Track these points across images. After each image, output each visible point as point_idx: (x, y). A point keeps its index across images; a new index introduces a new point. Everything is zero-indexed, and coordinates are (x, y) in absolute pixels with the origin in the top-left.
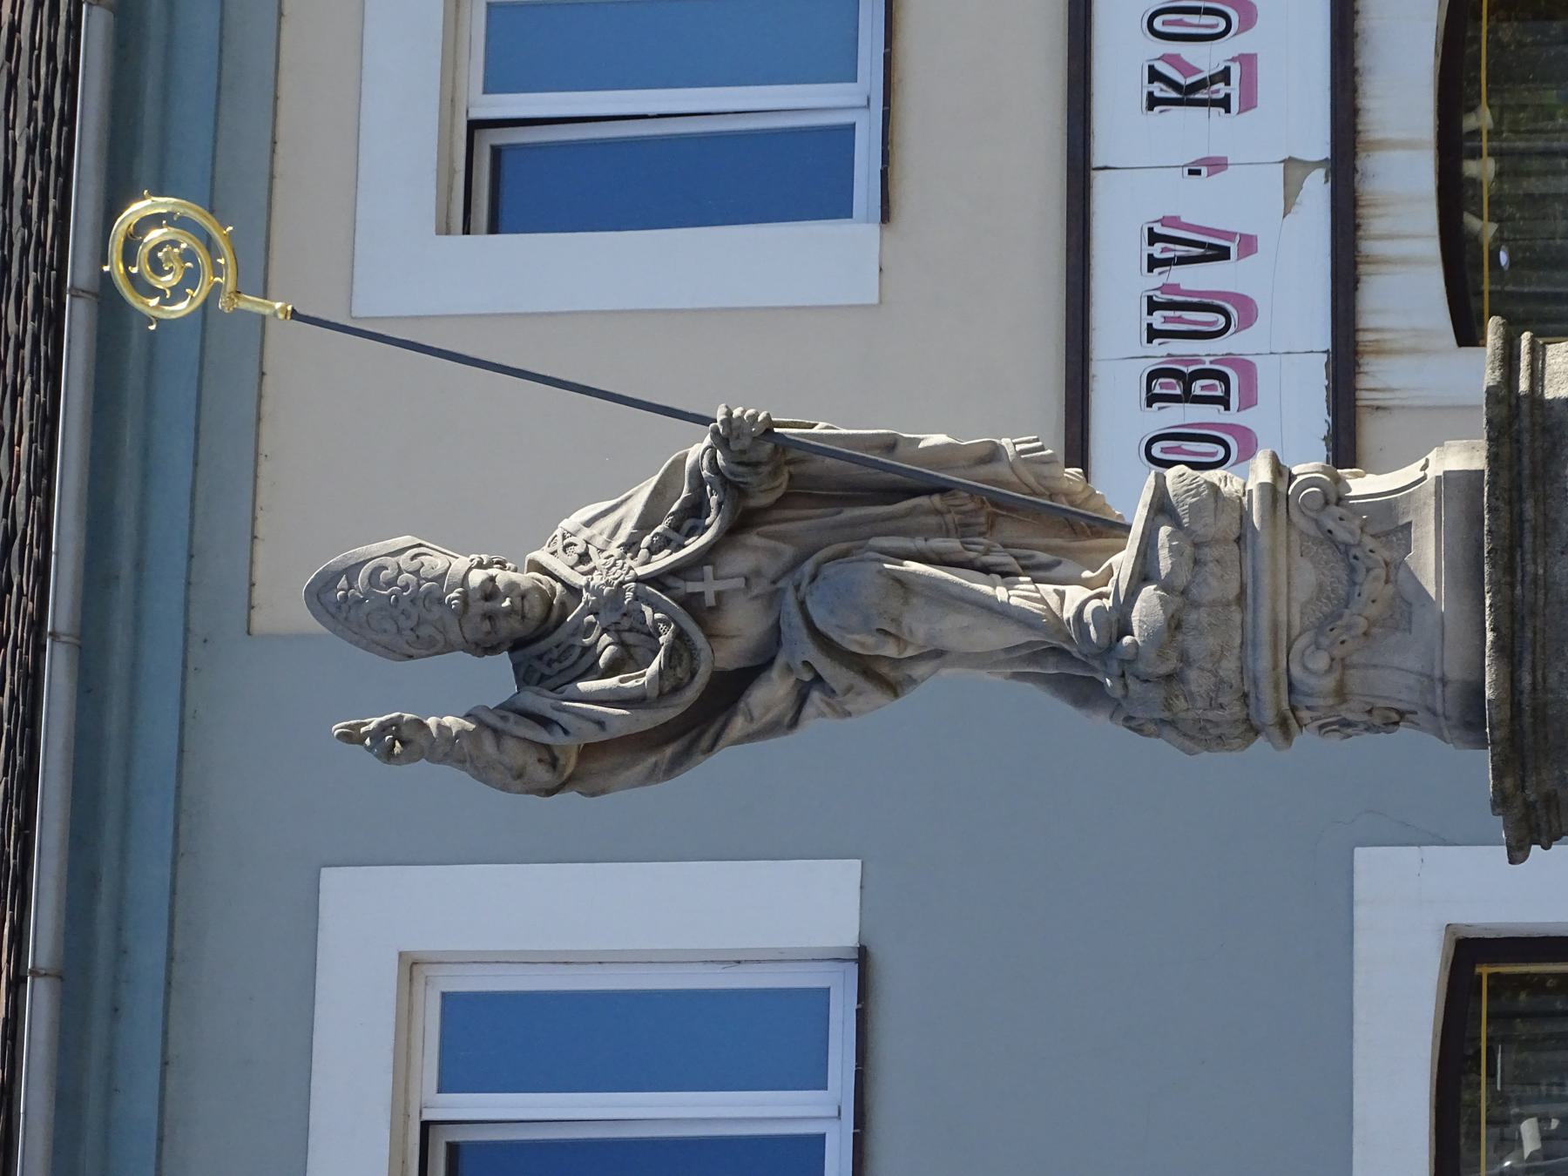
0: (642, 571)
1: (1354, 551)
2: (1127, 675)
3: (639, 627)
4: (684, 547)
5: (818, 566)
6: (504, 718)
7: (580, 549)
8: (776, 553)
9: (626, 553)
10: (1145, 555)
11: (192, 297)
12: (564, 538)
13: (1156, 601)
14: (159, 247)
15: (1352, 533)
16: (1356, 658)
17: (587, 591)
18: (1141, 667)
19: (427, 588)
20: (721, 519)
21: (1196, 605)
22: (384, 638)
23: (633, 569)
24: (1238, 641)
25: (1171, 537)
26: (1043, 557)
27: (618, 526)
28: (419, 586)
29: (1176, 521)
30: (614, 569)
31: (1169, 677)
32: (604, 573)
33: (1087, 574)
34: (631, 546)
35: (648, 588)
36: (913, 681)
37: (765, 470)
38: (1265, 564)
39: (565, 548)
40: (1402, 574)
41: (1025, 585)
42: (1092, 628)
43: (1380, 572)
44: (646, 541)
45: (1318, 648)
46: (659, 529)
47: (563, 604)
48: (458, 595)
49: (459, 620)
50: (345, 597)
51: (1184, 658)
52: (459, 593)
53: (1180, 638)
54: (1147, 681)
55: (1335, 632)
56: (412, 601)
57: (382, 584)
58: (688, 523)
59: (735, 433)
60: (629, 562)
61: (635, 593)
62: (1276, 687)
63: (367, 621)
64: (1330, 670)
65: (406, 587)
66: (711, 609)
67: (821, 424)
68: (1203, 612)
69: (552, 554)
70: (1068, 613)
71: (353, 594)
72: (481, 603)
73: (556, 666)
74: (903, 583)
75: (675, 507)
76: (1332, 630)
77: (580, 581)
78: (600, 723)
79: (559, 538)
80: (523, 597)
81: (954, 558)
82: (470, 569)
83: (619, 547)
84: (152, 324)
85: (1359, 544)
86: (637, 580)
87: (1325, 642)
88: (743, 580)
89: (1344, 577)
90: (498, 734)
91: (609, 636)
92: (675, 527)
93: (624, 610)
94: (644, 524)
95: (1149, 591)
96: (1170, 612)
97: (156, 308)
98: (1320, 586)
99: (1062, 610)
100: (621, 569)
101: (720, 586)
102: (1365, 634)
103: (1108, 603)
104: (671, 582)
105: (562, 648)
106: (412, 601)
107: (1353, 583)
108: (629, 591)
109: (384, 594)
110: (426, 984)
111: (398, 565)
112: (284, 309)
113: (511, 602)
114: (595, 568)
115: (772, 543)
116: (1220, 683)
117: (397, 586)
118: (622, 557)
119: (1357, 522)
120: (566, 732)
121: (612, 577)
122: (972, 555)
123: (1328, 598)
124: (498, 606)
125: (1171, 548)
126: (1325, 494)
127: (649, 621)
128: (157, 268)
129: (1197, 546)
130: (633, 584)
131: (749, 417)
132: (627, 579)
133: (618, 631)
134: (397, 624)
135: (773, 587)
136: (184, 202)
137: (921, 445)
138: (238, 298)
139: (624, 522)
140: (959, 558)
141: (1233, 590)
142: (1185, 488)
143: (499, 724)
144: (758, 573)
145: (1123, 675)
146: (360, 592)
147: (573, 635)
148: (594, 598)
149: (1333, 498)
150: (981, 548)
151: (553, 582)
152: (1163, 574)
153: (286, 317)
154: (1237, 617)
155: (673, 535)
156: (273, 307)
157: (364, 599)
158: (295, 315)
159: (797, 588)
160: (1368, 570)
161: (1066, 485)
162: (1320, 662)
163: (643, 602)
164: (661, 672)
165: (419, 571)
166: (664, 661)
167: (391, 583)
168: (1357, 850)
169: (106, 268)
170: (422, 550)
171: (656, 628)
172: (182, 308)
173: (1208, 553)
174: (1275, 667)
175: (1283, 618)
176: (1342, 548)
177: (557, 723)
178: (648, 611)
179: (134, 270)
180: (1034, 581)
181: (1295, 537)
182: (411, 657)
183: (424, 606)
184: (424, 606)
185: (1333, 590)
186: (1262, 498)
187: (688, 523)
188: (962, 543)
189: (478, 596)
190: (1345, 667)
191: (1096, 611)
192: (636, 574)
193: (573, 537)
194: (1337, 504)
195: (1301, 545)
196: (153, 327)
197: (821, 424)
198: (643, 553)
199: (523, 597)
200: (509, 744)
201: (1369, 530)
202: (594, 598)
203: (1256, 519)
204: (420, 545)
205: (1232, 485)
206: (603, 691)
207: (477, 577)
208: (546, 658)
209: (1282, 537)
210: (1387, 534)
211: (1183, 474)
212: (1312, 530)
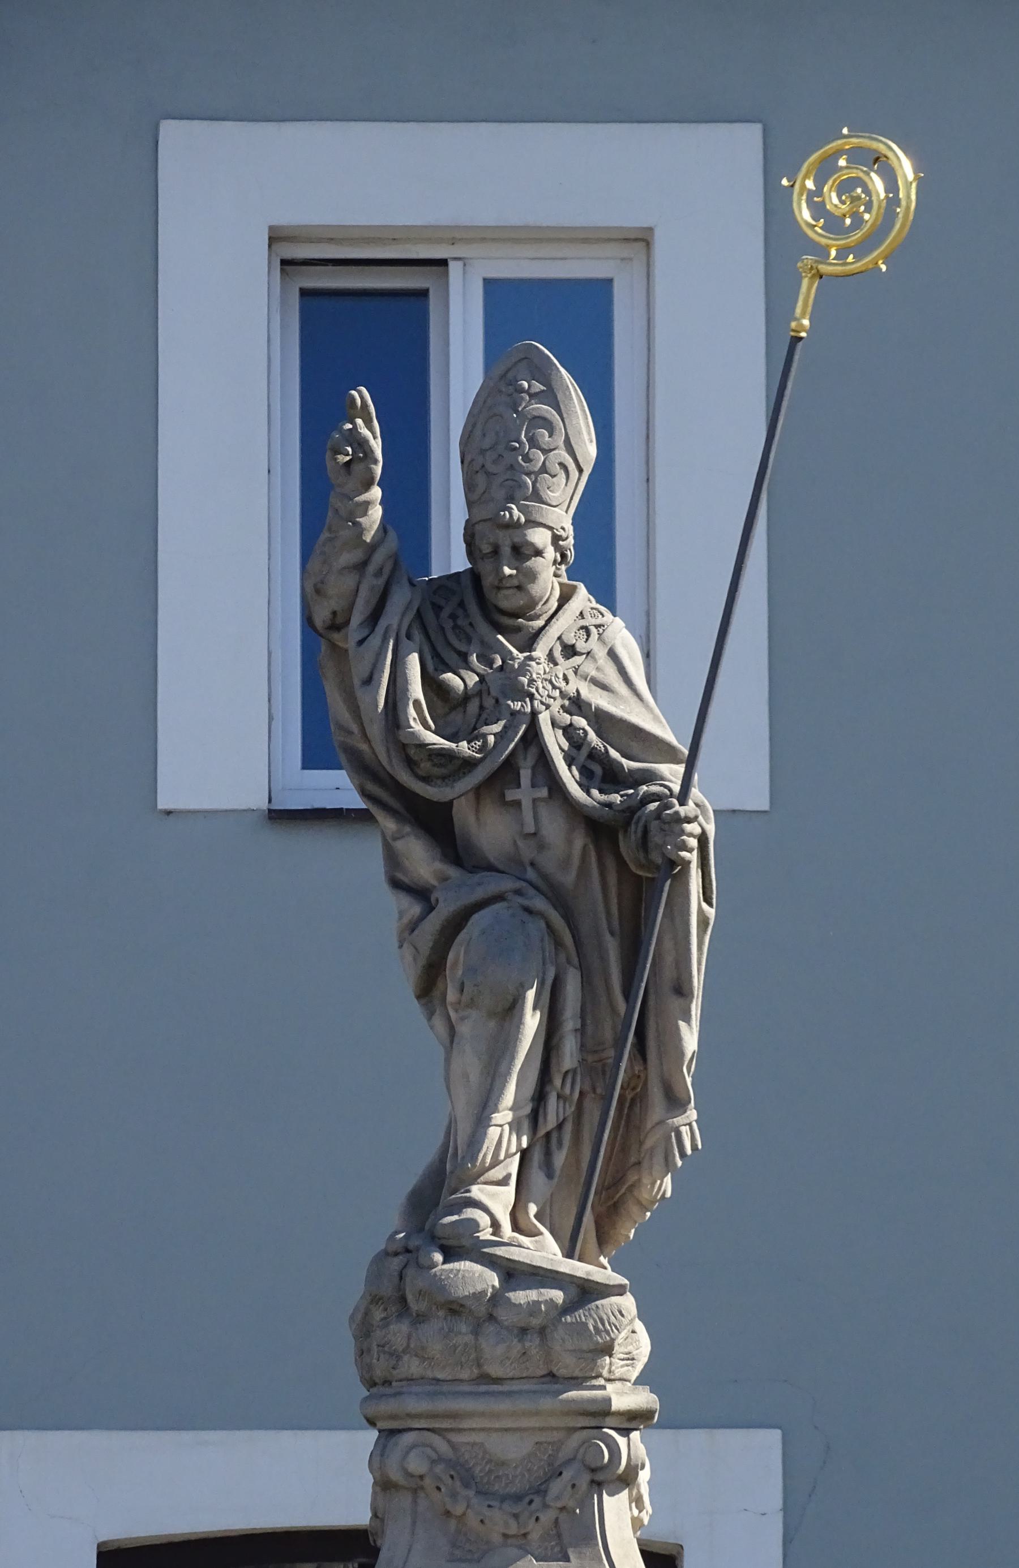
1: (537, 1500)
2: (408, 1255)
3: (484, 716)
4: (569, 766)
5: (541, 915)
6: (379, 573)
7: (581, 646)
9: (570, 699)
10: (534, 1274)
11: (815, 226)
12: (597, 626)
13: (479, 1288)
14: (867, 191)
15: (558, 1498)
16: (423, 1503)
17: (526, 658)
18: (410, 1272)
19: (525, 483)
20: (594, 807)
21: (476, 1332)
22: (478, 432)
23: (546, 709)
24: (440, 1376)
25: (551, 1302)
26: (560, 1158)
27: (604, 687)
28: (528, 474)
29: (569, 1308)
30: (550, 687)
31: (403, 1300)
32: (545, 676)
33: (533, 1209)
34: (577, 705)
35: (524, 727)
36: (430, 1015)
37: (641, 856)
38: (523, 1404)
39: (586, 629)
40: (513, 1552)
41: (515, 1143)
42: (455, 1218)
43: (513, 1529)
44: (581, 722)
45: (433, 1462)
46: (592, 736)
47: (519, 629)
48: (515, 518)
49: (490, 519)
50: (522, 390)
51: (420, 1319)
52: (519, 519)
53: (441, 1313)
54: (401, 1277)
55: (450, 1481)
56: (512, 466)
57: (533, 431)
58: (598, 770)
59: (666, 827)
60: (556, 706)
62: (393, 1417)
63: (495, 415)
64: (409, 1475)
65: (527, 459)
66: (503, 795)
67: (711, 912)
68: (469, 1338)
69: (581, 613)
70: (476, 1191)
71: (522, 398)
72: (508, 542)
73: (448, 625)
74: (512, 1010)
75: (614, 754)
76: (452, 1477)
77: (540, 652)
78: (370, 680)
79: (599, 620)
80: (519, 588)
81: (554, 1061)
82: (550, 528)
83: (578, 691)
84: (789, 181)
85: (546, 1506)
86: (534, 714)
87: (439, 1469)
88: (532, 831)
89: (512, 1489)
90: (361, 566)
91: (476, 683)
92: (593, 755)
93: (501, 700)
94: (601, 720)
95: (493, 1279)
96: (468, 1303)
97: (803, 186)
98: (503, 1464)
99: (486, 1183)
100: (549, 696)
102: (448, 1513)
103: (486, 1235)
104: (533, 751)
105: (469, 629)
106: (512, 466)
107: (503, 1499)
108: (522, 706)
109: (520, 434)
110: (623, 259)
113: (510, 576)
114: (556, 664)
115: (576, 861)
116: (396, 1356)
117: (529, 449)
118: (563, 695)
119: (571, 1504)
120: (361, 642)
121: (540, 686)
122: (558, 1082)
123: (490, 1471)
124: (505, 562)
125: (537, 1303)
126: (603, 1468)
127: (485, 729)
128: (845, 188)
129: (542, 1331)
130: (528, 709)
131: (683, 841)
132: (536, 703)
133: (479, 694)
134: (490, 448)
135: (527, 861)
136: (911, 217)
137: (682, 1024)
138: (813, 276)
139: (610, 694)
140: (554, 1069)
141: (494, 1370)
142: (605, 1317)
143: (371, 568)
144: (542, 847)
145: (408, 1251)
146: (525, 407)
147: (483, 643)
148: (516, 666)
149: (600, 1477)
150: (567, 1090)
151: (546, 617)
152: (511, 1295)
153: (793, 331)
154: (465, 1375)
155: (584, 752)
156: (803, 316)
157: (516, 412)
159: (518, 892)
160: (516, 1516)
161: (646, 1180)
162: (416, 1464)
163: (508, 721)
164: (423, 746)
165: (547, 473)
166: (436, 749)
167: (533, 442)
168: (776, 1435)
169: (845, 131)
170: (574, 473)
171: (477, 738)
172: (906, 168)
173: (532, 1344)
174: (410, 1416)
175: (466, 1424)
176: (543, 1487)
177: (372, 631)
178: (497, 728)
179: (842, 162)
180: (525, 1154)
181: (556, 1436)
182: (462, 462)
183: (507, 480)
185: (497, 1477)
186: (593, 1401)
187: (598, 770)
188: (574, 1071)
189: (516, 540)
190: (415, 1491)
191: (474, 1225)
192: (540, 713)
193: (597, 636)
194: (593, 1482)
195: (549, 1443)
196: (785, 182)
197: (711, 912)
198: (566, 718)
200: (349, 581)
201: (563, 1517)
202: (516, 666)
203: (573, 1394)
204: (581, 471)
205: (622, 1366)
206: (406, 682)
207: (540, 537)
208: (460, 612)
209: (554, 1422)
210: (559, 1536)
211: (623, 1315)
212: (563, 1455)
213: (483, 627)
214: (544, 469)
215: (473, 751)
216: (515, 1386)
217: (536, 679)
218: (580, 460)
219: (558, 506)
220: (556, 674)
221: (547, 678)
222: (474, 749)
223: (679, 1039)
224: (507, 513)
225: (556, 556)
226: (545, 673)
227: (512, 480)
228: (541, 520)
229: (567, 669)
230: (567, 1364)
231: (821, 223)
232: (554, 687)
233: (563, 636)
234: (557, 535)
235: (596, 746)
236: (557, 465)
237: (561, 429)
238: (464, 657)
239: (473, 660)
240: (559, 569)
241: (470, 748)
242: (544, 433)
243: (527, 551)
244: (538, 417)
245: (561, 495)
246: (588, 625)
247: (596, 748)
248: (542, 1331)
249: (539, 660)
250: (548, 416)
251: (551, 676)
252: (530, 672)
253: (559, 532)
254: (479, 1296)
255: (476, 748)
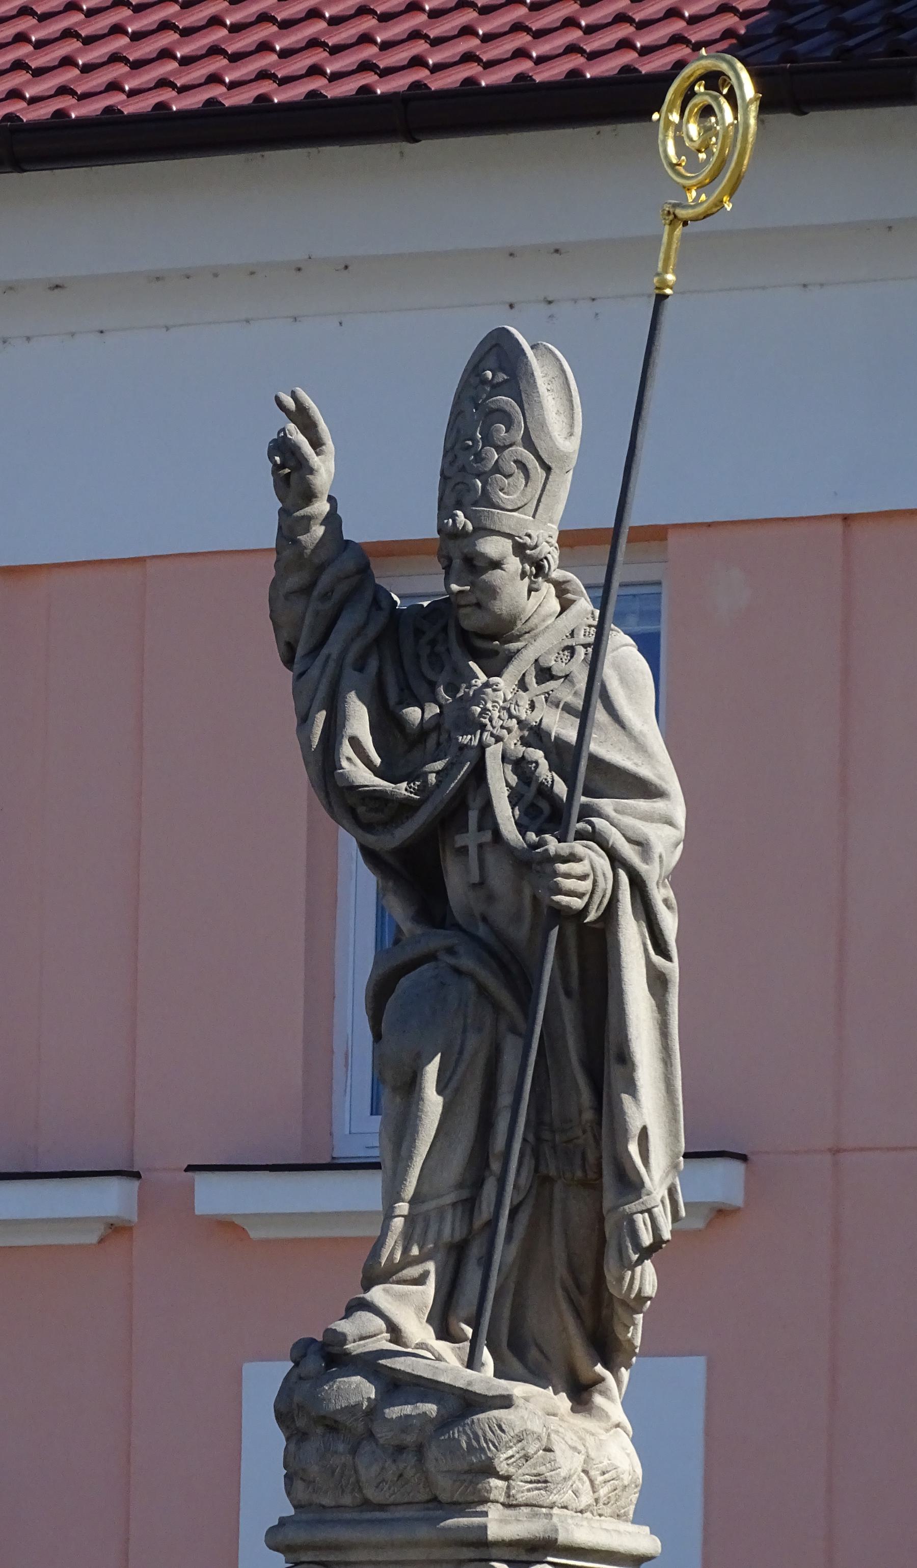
0: (493, 753)
5: (472, 976)
6: (325, 597)
7: (559, 668)
8: (517, 918)
10: (418, 1385)
13: (353, 1400)
19: (475, 485)
28: (478, 476)
29: (445, 1423)
30: (505, 715)
38: (400, 1534)
44: (538, 755)
50: (485, 381)
53: (320, 1430)
56: (464, 466)
58: (544, 806)
61: (466, 745)
65: (479, 458)
80: (478, 605)
86: (482, 747)
90: (307, 590)
95: (369, 1391)
96: (339, 1417)
99: (393, 1283)
101: (473, 852)
111: (511, 445)
112: (664, 284)
113: (461, 592)
117: (482, 448)
130: (475, 743)
131: (557, 883)
137: (626, 1098)
141: (371, 1494)
142: (480, 1433)
143: (316, 593)
144: (491, 898)
148: (471, 693)
154: (347, 1500)
155: (534, 788)
156: (666, 271)
158: (661, 298)
159: (451, 951)
167: (488, 440)
170: (538, 473)
171: (417, 779)
173: (408, 1462)
178: (439, 765)
179: (700, 88)
183: (458, 484)
184: (458, 484)
186: (469, 1528)
192: (489, 746)
199: (478, 605)
204: (548, 469)
205: (529, 1490)
207: (492, 547)
209: (436, 1554)
211: (503, 1431)
213: (457, 651)
214: (497, 469)
215: (411, 792)
216: (399, 1513)
217: (491, 708)
218: (544, 456)
219: (519, 508)
220: (517, 701)
221: (506, 706)
222: (412, 790)
223: (623, 1113)
224: (450, 520)
225: (523, 568)
226: (505, 701)
227: (462, 483)
228: (492, 527)
229: (537, 696)
230: (445, 1488)
231: (683, 160)
232: (511, 716)
233: (540, 660)
234: (520, 543)
235: (544, 781)
236: (512, 463)
237: (520, 423)
238: (433, 686)
239: (440, 690)
240: (535, 582)
241: (408, 788)
242: (501, 428)
243: (479, 563)
244: (497, 410)
245: (518, 497)
246: (574, 644)
247: (544, 783)
248: (420, 1450)
249: (497, 686)
250: (507, 409)
251: (511, 704)
252: (484, 700)
253: (523, 539)
254: (353, 1409)
255: (414, 789)
